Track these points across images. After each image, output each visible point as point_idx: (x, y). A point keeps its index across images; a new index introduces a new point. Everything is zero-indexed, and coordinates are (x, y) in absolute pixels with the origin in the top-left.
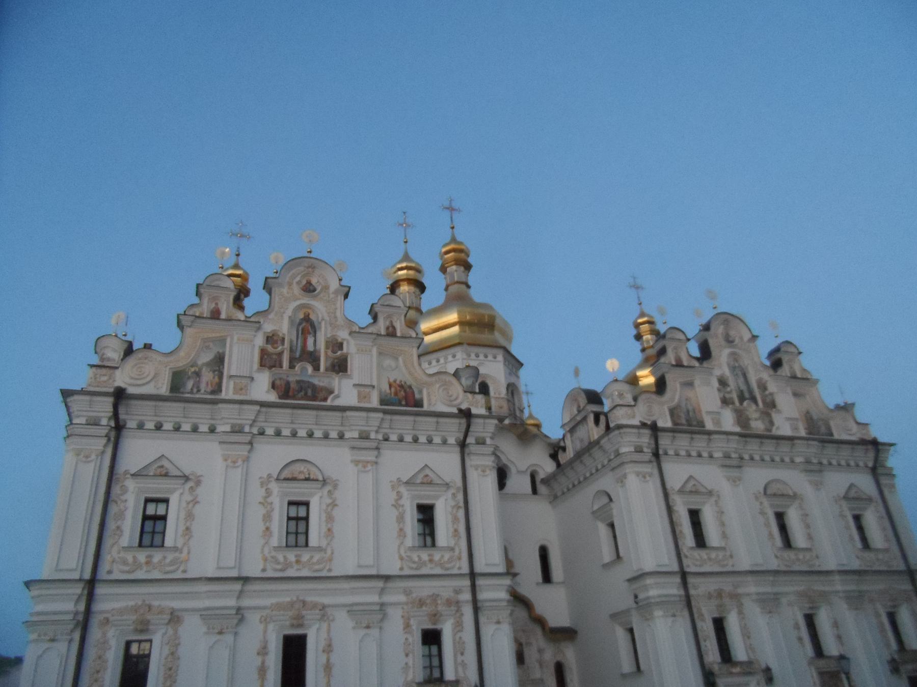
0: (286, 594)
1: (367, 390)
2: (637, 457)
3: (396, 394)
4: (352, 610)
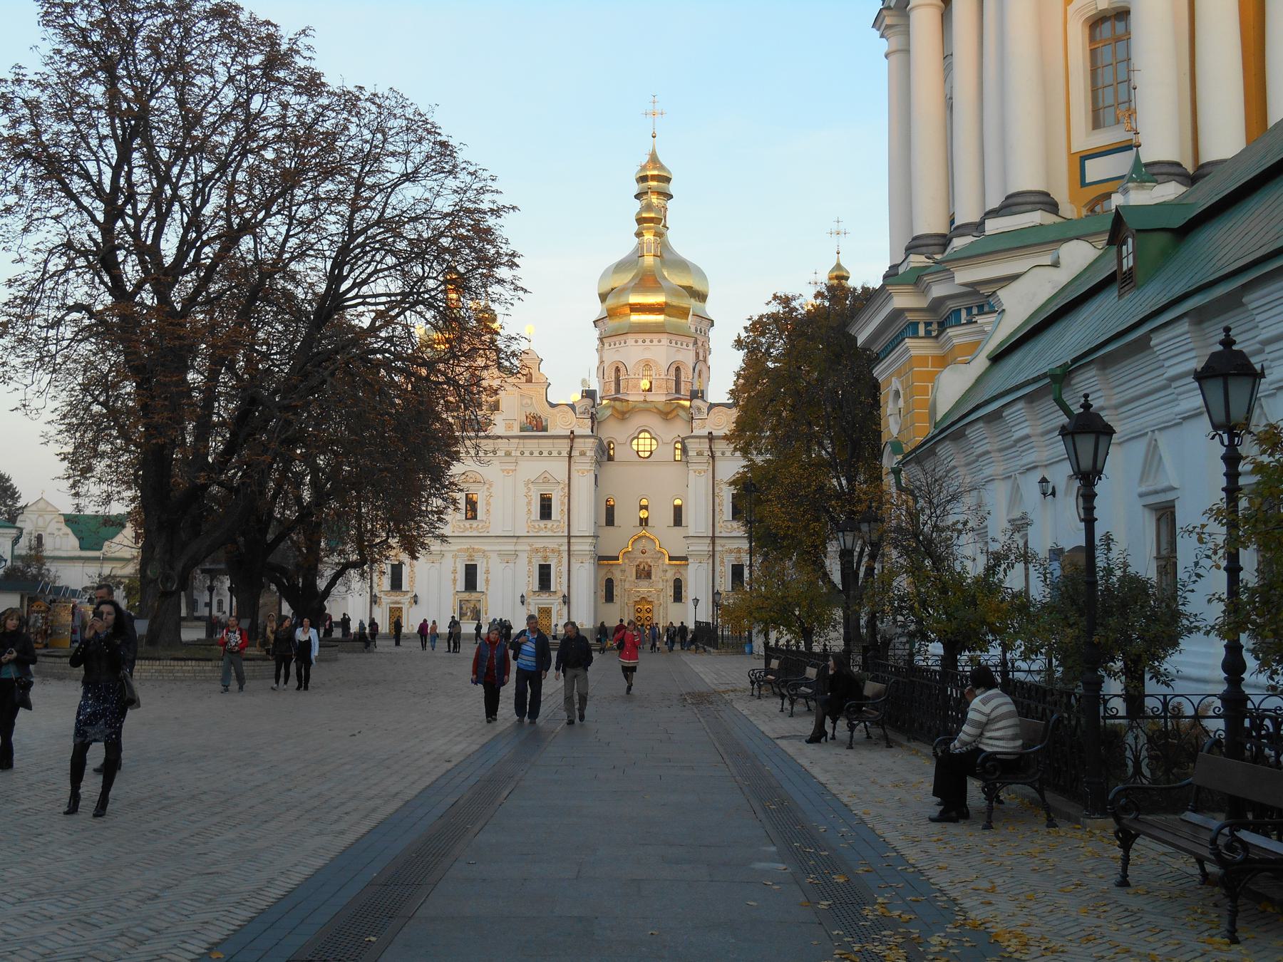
0: (465, 544)
1: (511, 422)
2: (700, 459)
3: (530, 423)
4: (500, 554)
